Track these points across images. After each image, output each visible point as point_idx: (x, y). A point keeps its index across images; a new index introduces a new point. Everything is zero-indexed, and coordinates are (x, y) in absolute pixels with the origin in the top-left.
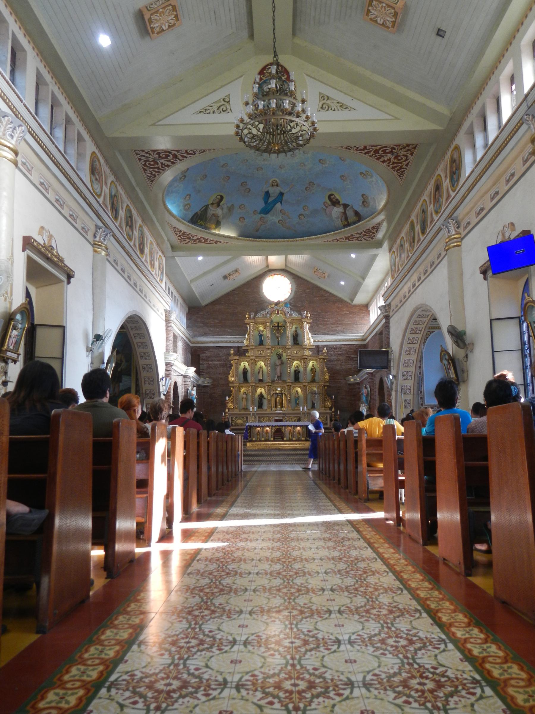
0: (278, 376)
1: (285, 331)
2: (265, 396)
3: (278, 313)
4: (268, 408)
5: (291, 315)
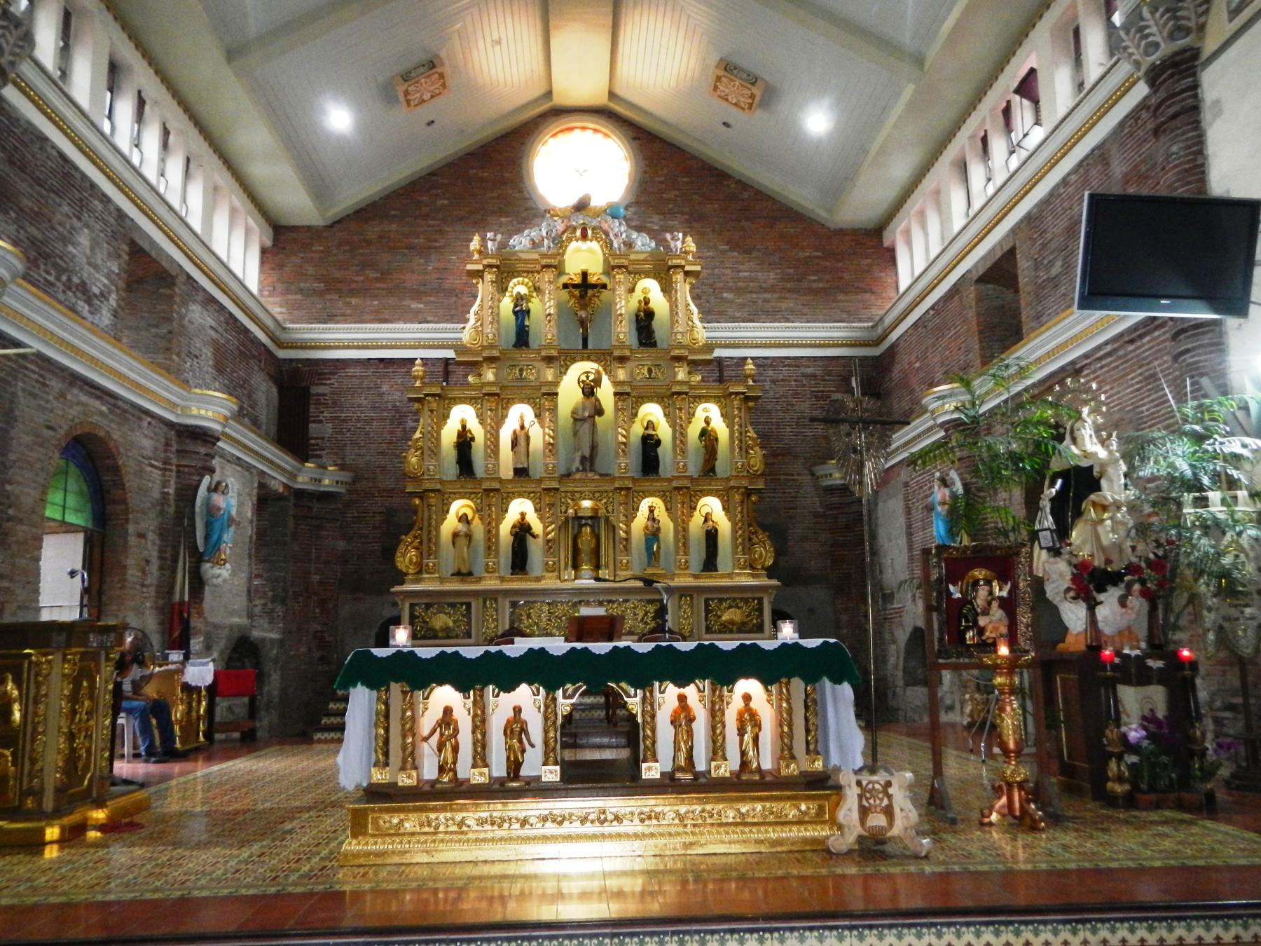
0: (583, 459)
1: (609, 308)
2: (537, 526)
3: (584, 237)
4: (547, 568)
5: (629, 245)
